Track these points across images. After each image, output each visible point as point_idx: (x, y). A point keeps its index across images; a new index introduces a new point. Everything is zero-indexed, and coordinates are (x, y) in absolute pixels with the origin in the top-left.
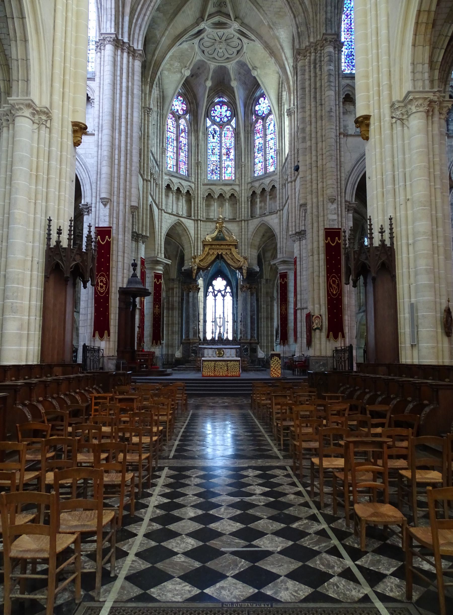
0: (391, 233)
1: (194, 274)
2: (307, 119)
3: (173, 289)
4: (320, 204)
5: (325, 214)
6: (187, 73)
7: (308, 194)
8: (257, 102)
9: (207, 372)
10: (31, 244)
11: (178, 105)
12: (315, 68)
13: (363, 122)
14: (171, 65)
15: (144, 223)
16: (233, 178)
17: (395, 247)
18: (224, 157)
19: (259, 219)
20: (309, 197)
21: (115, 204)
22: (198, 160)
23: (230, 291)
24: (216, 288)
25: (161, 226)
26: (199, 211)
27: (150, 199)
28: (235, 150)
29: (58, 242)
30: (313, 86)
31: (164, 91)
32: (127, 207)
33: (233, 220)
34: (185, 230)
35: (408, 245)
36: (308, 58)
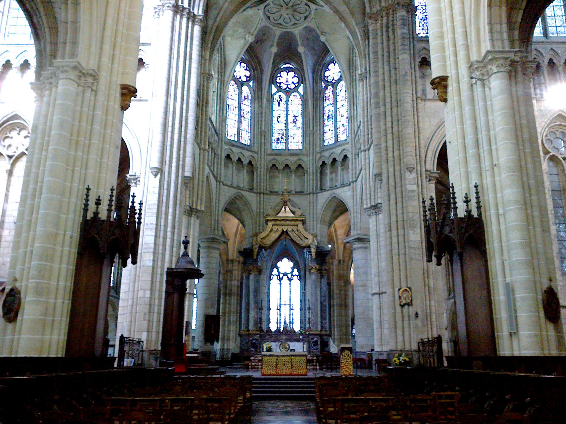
0: (478, 203)
1: (255, 253)
2: (381, 83)
3: (231, 272)
4: (397, 173)
5: (403, 185)
6: (251, 39)
7: (383, 163)
8: (326, 68)
9: (268, 370)
10: (65, 216)
11: (241, 71)
12: (387, 31)
13: (441, 84)
14: (234, 31)
15: (200, 196)
17: (483, 218)
18: (291, 125)
19: (329, 192)
20: (384, 166)
21: (166, 174)
22: (261, 128)
23: (297, 274)
24: (282, 270)
25: (219, 200)
26: (262, 184)
27: (207, 170)
28: (303, 118)
29: (96, 214)
30: (385, 50)
31: (227, 56)
32: (180, 178)
33: (301, 193)
34: (247, 203)
35: (498, 215)
36: (380, 22)
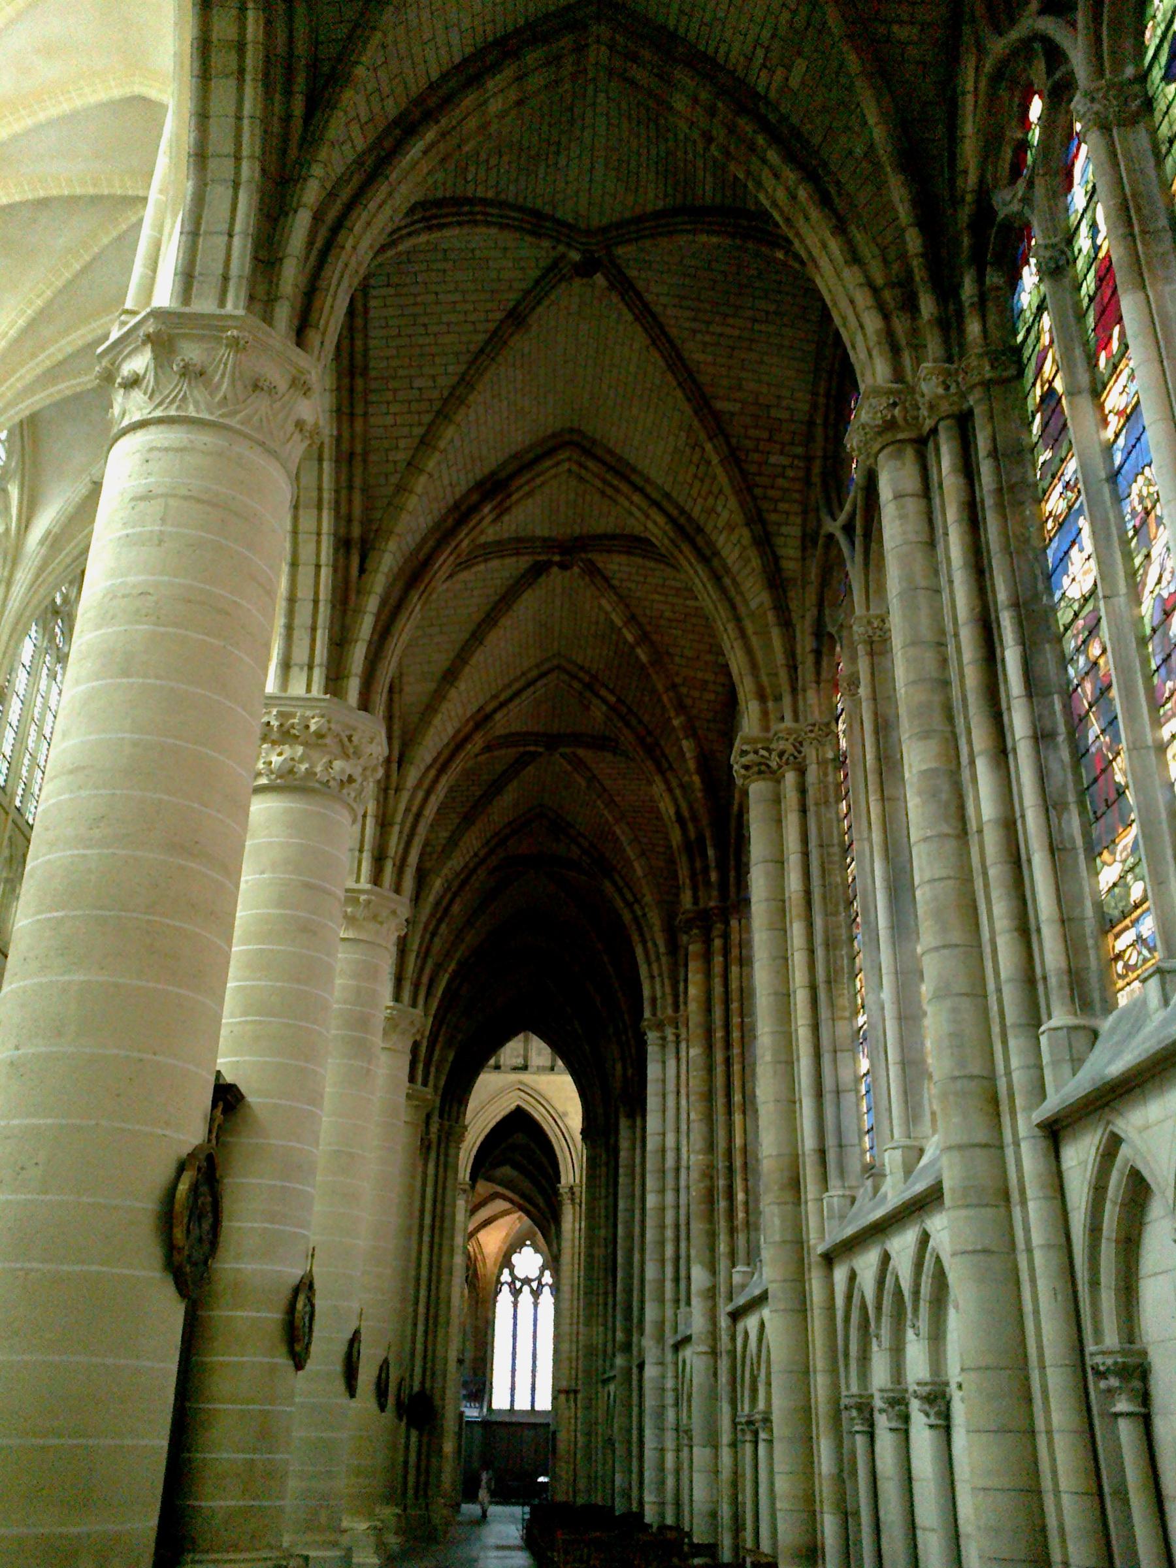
23: (550, 1281)
24: (520, 1273)
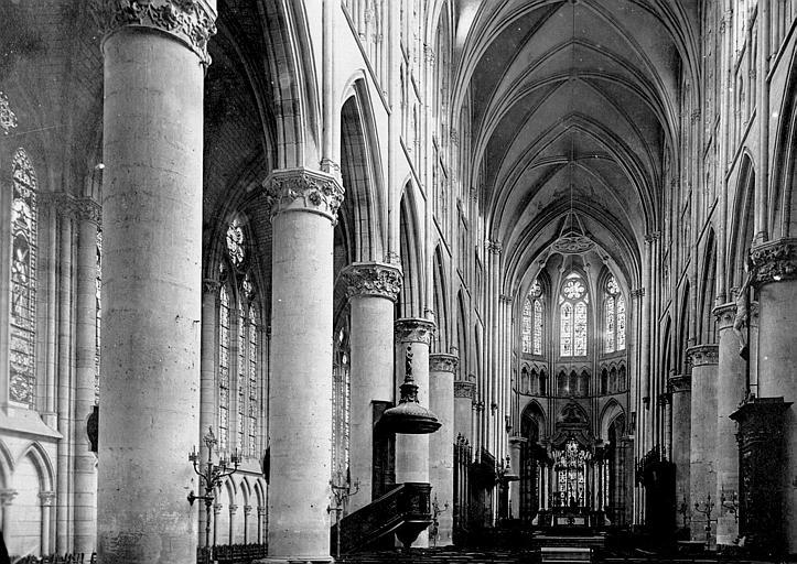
16: (585, 354)
